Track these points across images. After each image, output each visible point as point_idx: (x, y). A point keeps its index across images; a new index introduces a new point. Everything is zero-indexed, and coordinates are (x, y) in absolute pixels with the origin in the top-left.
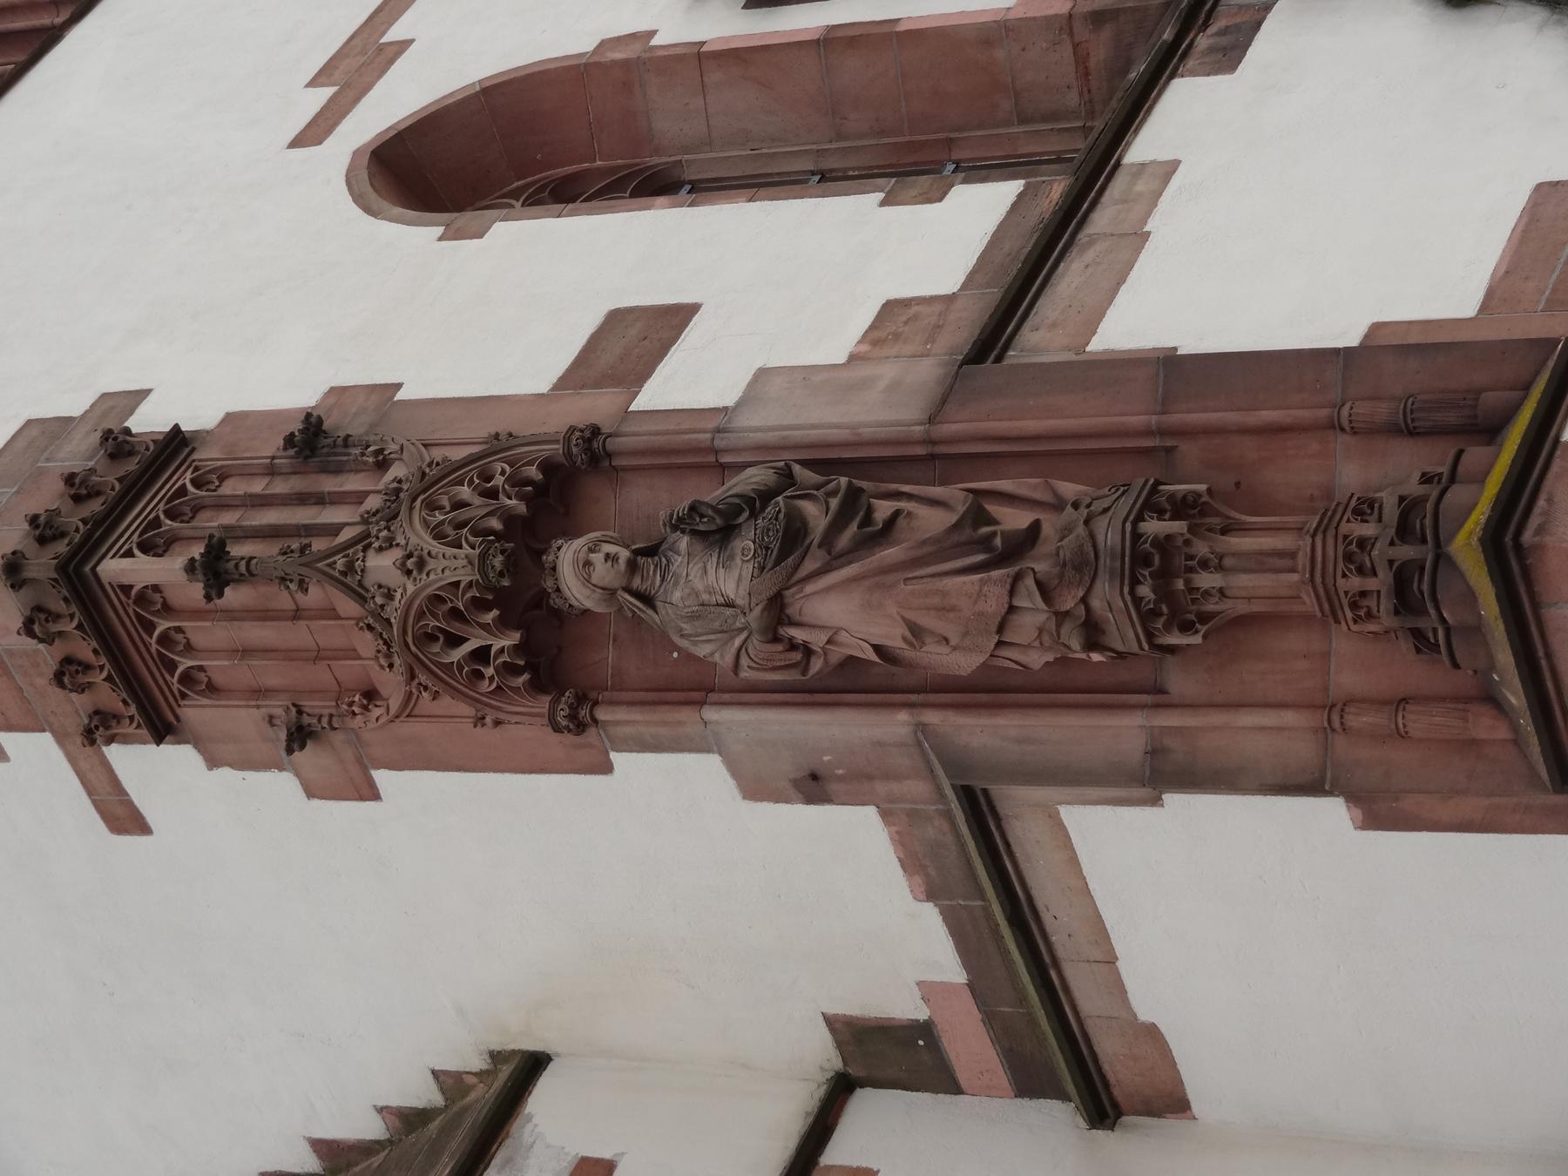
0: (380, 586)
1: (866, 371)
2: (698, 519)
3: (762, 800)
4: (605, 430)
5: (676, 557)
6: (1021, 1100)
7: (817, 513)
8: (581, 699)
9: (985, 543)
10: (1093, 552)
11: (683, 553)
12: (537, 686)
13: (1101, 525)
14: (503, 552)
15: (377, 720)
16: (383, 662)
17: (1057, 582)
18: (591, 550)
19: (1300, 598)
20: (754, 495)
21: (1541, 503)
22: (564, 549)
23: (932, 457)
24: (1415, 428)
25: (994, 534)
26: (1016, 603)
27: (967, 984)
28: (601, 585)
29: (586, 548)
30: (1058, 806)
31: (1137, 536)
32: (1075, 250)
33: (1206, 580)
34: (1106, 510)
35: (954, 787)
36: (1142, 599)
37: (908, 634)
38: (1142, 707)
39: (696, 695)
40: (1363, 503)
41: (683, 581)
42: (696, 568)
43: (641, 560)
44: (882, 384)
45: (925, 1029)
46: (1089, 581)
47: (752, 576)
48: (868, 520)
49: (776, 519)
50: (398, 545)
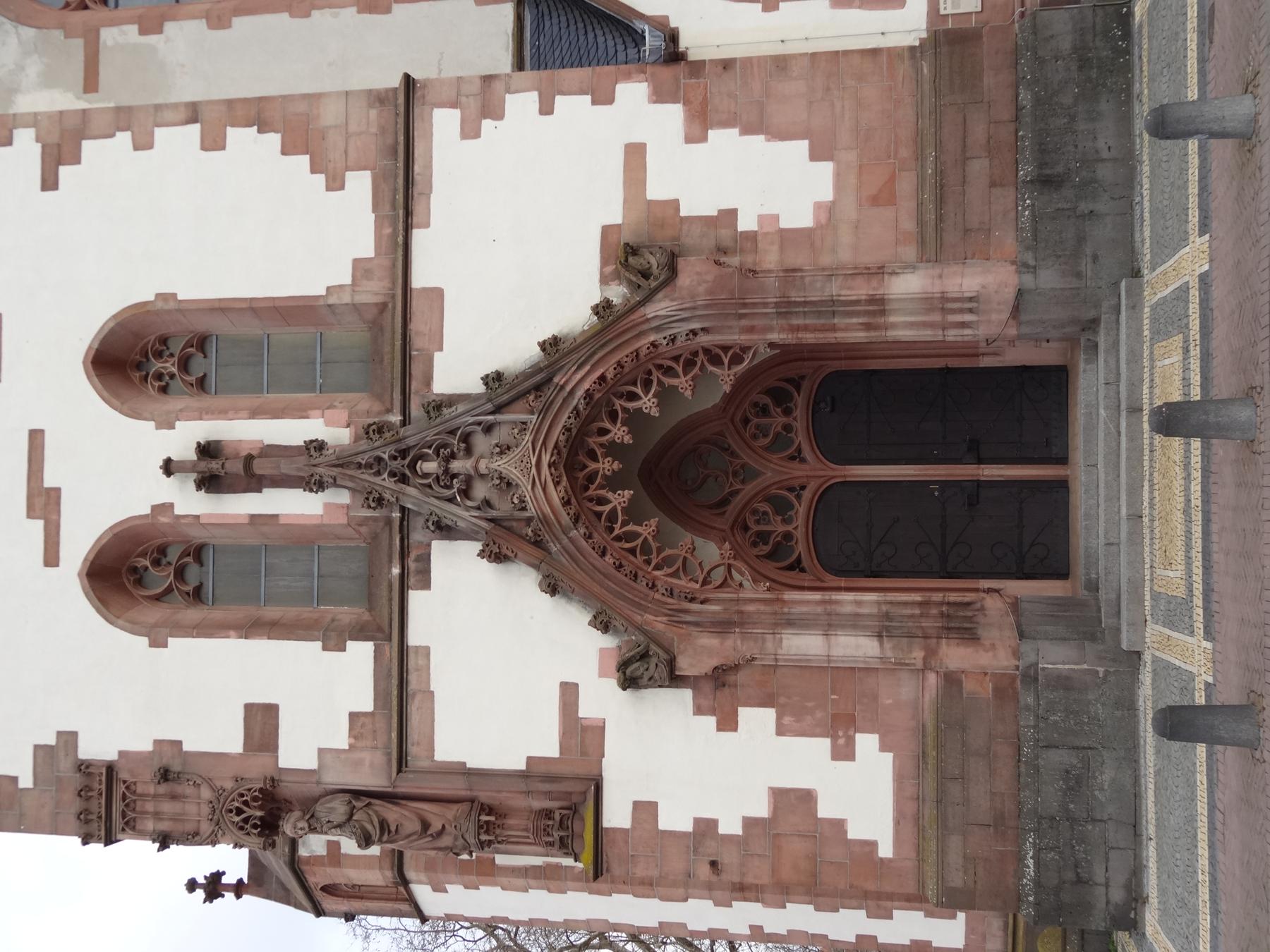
1: (357, 755)
4: (276, 778)
9: (431, 835)
21: (604, 856)
43: (312, 821)
44: (367, 763)
48: (390, 832)
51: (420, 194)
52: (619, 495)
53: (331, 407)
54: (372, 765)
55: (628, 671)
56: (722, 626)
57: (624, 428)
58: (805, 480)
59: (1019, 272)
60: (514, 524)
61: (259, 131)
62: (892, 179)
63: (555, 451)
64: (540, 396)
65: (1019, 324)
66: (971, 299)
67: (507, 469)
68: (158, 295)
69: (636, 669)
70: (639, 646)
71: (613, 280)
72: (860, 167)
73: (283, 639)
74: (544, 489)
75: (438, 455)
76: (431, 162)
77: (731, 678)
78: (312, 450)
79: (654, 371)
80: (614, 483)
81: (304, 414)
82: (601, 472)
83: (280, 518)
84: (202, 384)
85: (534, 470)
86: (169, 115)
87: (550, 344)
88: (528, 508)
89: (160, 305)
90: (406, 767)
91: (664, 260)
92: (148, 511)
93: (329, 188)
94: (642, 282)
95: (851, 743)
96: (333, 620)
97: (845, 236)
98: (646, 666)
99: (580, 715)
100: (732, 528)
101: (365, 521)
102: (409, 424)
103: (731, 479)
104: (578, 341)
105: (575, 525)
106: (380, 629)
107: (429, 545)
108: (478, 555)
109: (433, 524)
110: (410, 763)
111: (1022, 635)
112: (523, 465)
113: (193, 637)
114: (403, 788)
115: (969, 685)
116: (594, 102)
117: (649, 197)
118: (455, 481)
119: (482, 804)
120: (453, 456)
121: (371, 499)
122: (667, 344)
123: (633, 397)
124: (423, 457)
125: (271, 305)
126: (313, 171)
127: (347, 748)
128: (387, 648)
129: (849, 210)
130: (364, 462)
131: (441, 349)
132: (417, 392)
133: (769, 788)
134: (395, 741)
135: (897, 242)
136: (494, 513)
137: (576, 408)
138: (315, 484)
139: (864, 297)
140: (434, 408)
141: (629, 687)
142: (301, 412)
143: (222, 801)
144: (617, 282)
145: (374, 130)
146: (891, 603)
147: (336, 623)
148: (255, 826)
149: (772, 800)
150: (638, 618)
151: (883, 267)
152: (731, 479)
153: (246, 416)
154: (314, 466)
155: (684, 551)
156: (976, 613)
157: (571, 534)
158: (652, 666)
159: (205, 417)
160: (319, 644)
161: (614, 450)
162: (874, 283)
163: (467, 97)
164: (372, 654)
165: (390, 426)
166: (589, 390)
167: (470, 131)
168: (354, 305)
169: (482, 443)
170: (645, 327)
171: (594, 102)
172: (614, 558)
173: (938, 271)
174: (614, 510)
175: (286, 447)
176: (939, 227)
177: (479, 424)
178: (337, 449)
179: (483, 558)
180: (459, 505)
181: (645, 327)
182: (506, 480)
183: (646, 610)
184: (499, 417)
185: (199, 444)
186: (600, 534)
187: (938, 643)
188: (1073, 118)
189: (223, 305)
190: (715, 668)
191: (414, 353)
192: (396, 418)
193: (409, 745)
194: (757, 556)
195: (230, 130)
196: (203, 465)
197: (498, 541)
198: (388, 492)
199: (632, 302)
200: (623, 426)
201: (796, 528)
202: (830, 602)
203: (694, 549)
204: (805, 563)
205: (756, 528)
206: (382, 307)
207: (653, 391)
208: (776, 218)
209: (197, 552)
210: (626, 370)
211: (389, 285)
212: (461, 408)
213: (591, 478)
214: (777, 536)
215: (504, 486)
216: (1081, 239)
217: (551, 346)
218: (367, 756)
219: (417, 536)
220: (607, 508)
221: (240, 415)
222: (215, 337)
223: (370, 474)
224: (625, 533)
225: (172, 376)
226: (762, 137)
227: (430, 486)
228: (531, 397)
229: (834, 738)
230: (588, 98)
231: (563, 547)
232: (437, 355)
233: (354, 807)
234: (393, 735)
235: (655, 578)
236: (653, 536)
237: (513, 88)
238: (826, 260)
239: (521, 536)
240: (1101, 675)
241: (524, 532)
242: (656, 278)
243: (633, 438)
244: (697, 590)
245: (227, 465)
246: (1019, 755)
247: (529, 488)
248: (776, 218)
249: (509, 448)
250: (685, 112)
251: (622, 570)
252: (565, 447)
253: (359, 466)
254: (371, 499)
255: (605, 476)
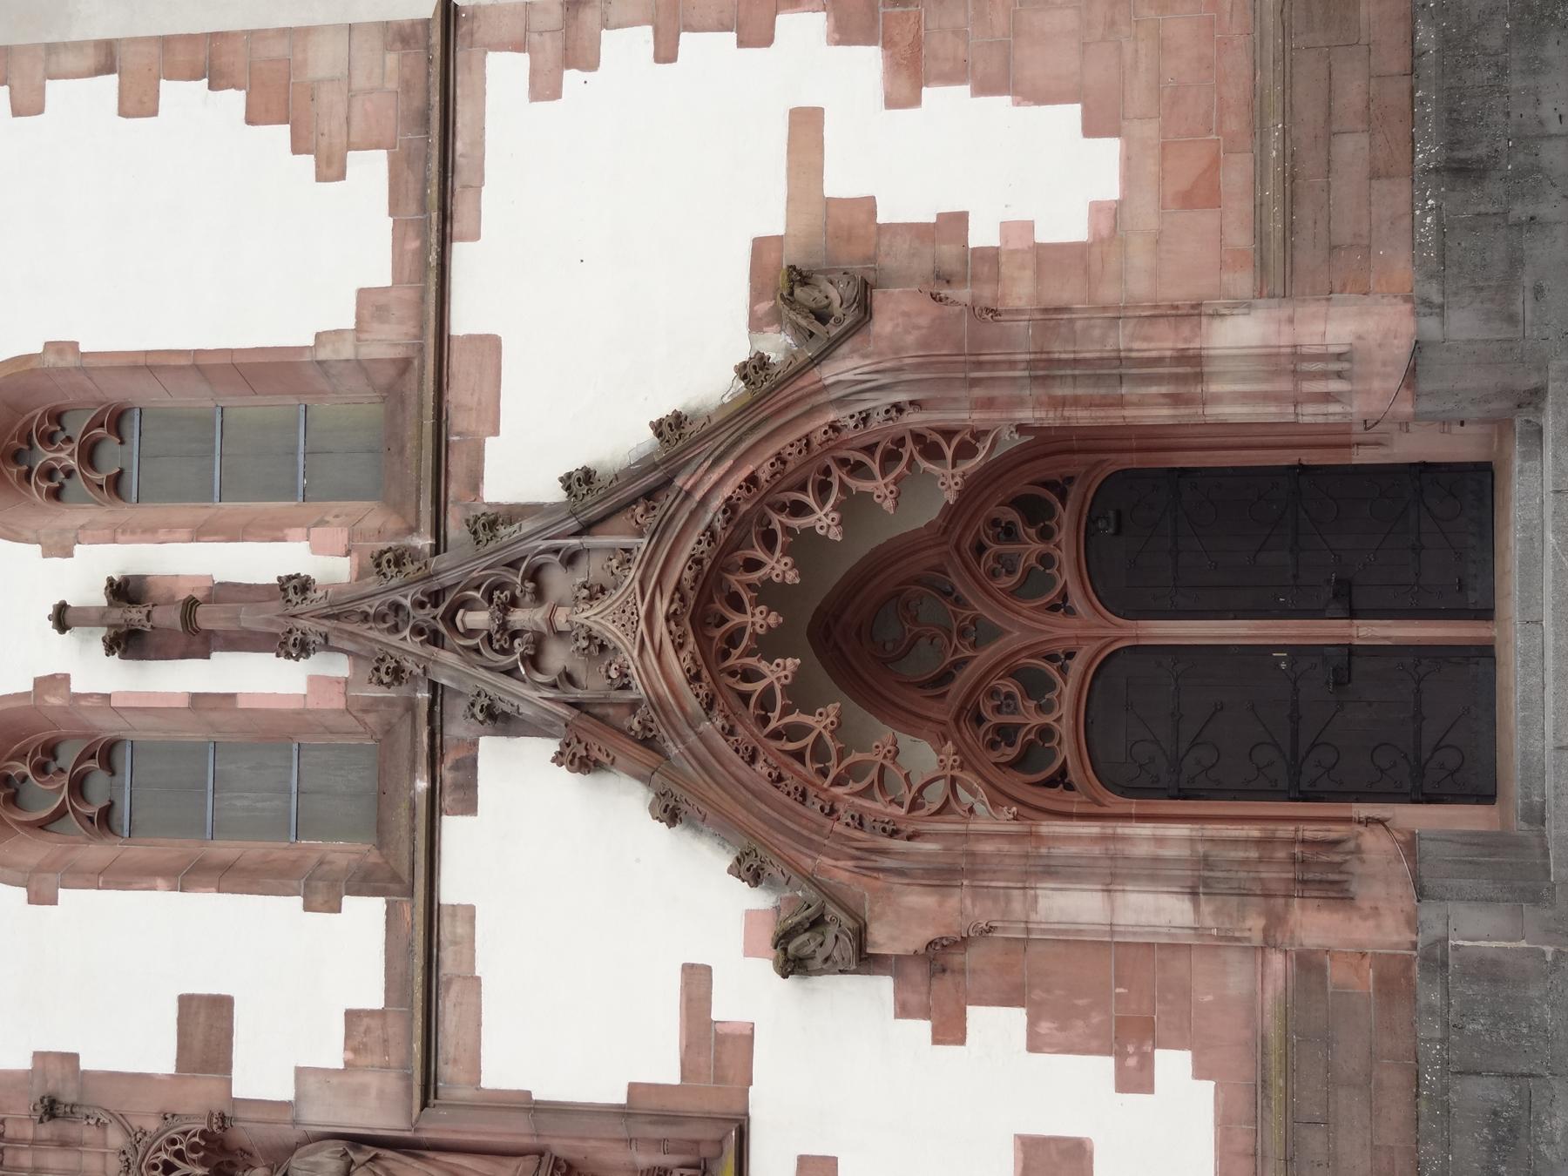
1: (358, 1079)
4: (227, 1115)
44: (373, 1092)
51: (464, 187)
52: (778, 665)
53: (321, 523)
54: (381, 1094)
55: (791, 948)
56: (942, 877)
57: (787, 560)
58: (1074, 642)
59: (1415, 313)
60: (611, 711)
61: (211, 87)
62: (1215, 165)
63: (677, 596)
64: (654, 508)
65: (1417, 396)
66: (1339, 357)
67: (600, 624)
68: (48, 345)
69: (803, 945)
70: (809, 907)
71: (769, 324)
72: (1164, 147)
73: (242, 893)
74: (659, 656)
75: (491, 601)
76: (482, 136)
77: (955, 959)
78: (291, 591)
79: (834, 468)
80: (769, 646)
81: (280, 534)
82: (749, 630)
83: (239, 698)
84: (115, 485)
85: (642, 625)
86: (69, 61)
87: (670, 425)
88: (633, 685)
89: (51, 360)
90: (436, 1098)
91: (851, 292)
92: (28, 687)
93: (320, 178)
94: (816, 327)
95: (1147, 1063)
96: (321, 863)
97: (1140, 256)
98: (819, 939)
99: (714, 1017)
100: (957, 720)
101: (372, 705)
102: (445, 551)
103: (955, 641)
104: (715, 421)
105: (707, 714)
106: (396, 878)
107: (475, 744)
108: (553, 761)
109: (481, 711)
110: (441, 1092)
111: (1421, 893)
112: (625, 617)
113: (99, 888)
114: (429, 1133)
115: (1336, 973)
116: (741, 43)
117: (827, 193)
118: (517, 642)
119: (556, 1158)
120: (514, 602)
121: (383, 670)
122: (856, 427)
123: (800, 509)
124: (466, 604)
125: (227, 360)
126: (296, 150)
127: (341, 1066)
128: (407, 908)
129: (1146, 215)
130: (372, 611)
131: (496, 432)
132: (457, 501)
133: (1015, 1135)
134: (419, 1056)
135: (1222, 266)
136: (578, 694)
137: (709, 527)
138: (294, 645)
139: (1168, 353)
140: (484, 525)
141: (792, 972)
142: (273, 531)
143: (141, 1150)
144: (776, 327)
145: (392, 85)
146: (1212, 840)
147: (326, 867)
149: (1021, 1156)
150: (807, 863)
151: (1199, 305)
152: (955, 641)
153: (186, 537)
154: (294, 616)
155: (882, 755)
156: (1348, 857)
157: (701, 728)
158: (830, 940)
159: (120, 537)
160: (298, 901)
161: (769, 594)
162: (1186, 330)
163: (541, 33)
164: (383, 917)
165: (415, 554)
166: (730, 498)
167: (545, 88)
168: (359, 361)
169: (559, 581)
170: (821, 398)
171: (741, 43)
172: (770, 766)
173: (1286, 312)
174: (770, 689)
175: (249, 586)
176: (1289, 244)
177: (557, 551)
178: (330, 590)
179: (561, 764)
180: (523, 681)
181: (821, 398)
182: (598, 642)
183: (819, 849)
184: (588, 541)
185: (111, 581)
186: (746, 728)
187: (1287, 905)
188: (1502, 70)
189: (150, 361)
190: (930, 943)
191: (454, 438)
192: (424, 542)
193: (441, 1063)
194: (996, 764)
195: (164, 84)
196: (117, 615)
197: (586, 738)
198: (410, 658)
199: (801, 359)
200: (784, 554)
201: (1058, 720)
202: (1115, 838)
203: (897, 752)
204: (1074, 775)
205: (996, 719)
206: (404, 365)
207: (832, 501)
208: (1029, 226)
209: (106, 753)
210: (790, 467)
211: (414, 331)
212: (528, 526)
213: (733, 639)
214: (1029, 732)
215: (594, 650)
216: (1516, 262)
217: (671, 428)
218: (373, 1080)
219: (456, 728)
220: (758, 687)
221: (177, 536)
222: (137, 412)
223: (379, 630)
224: (786, 726)
225: (69, 473)
226: (1007, 100)
227: (477, 651)
228: (640, 510)
229: (1121, 1056)
230: (732, 37)
231: (689, 749)
232: (490, 443)
233: (352, 1161)
234: (415, 1046)
235: (834, 799)
236: (832, 732)
237: (613, 20)
238: (1109, 293)
239: (621, 731)
240: (1549, 958)
241: (626, 724)
242: (839, 322)
243: (800, 575)
244: (900, 817)
245: (156, 614)
246: (1418, 1086)
247: (635, 654)
248: (1029, 226)
249: (603, 590)
250: (885, 58)
251: (782, 784)
252: (692, 588)
253: (365, 617)
254: (383, 670)
255: (754, 635)
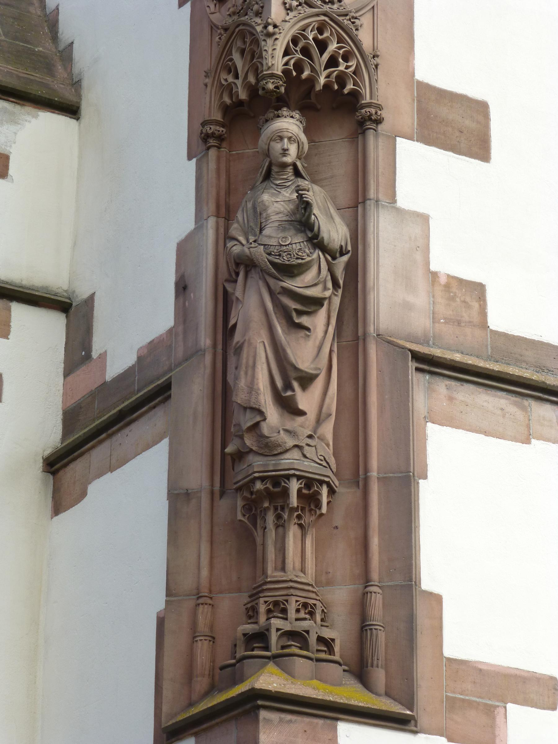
0: (262, 7)
1: (422, 284)
2: (303, 207)
3: (177, 255)
4: (380, 127)
5: (290, 192)
6: (62, 414)
7: (306, 281)
8: (220, 138)
9: (288, 386)
10: (277, 453)
11: (291, 196)
12: (226, 109)
13: (295, 454)
14: (277, 87)
15: (208, 6)
16: (231, 10)
17: (259, 434)
18: (290, 139)
19: (263, 575)
20: (319, 239)
21: (289, 717)
22: (291, 120)
23: (357, 338)
24: (366, 630)
25: (293, 390)
26: (248, 411)
27: (105, 382)
28: (270, 148)
29: (290, 135)
30: (168, 438)
31: (288, 477)
32: (514, 398)
33: (270, 518)
34: (305, 456)
35: (171, 377)
36: (254, 483)
37: (240, 343)
38: (212, 485)
39: (223, 210)
40: (312, 607)
41: (273, 200)
42: (280, 206)
43: (290, 170)
44: (411, 298)
45: (88, 357)
46: (260, 453)
47: (271, 245)
48: (300, 313)
49: (297, 258)
50: (288, 14)
54: (408, 306)
99: (510, 706)
110: (420, 375)
148: (298, 66)
193: (448, 382)
233: (334, 258)
